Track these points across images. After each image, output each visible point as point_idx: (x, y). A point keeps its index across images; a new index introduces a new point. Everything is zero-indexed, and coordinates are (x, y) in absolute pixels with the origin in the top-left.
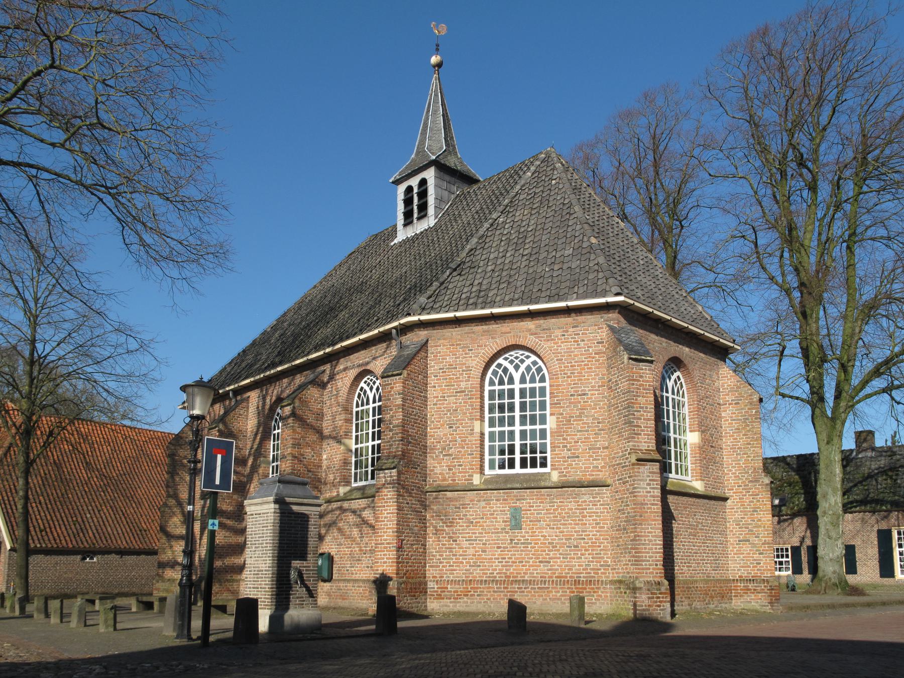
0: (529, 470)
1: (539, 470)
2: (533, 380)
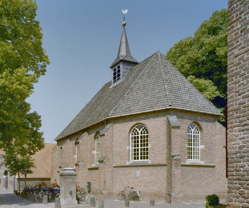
0: (143, 160)
1: (146, 160)
2: (144, 133)
